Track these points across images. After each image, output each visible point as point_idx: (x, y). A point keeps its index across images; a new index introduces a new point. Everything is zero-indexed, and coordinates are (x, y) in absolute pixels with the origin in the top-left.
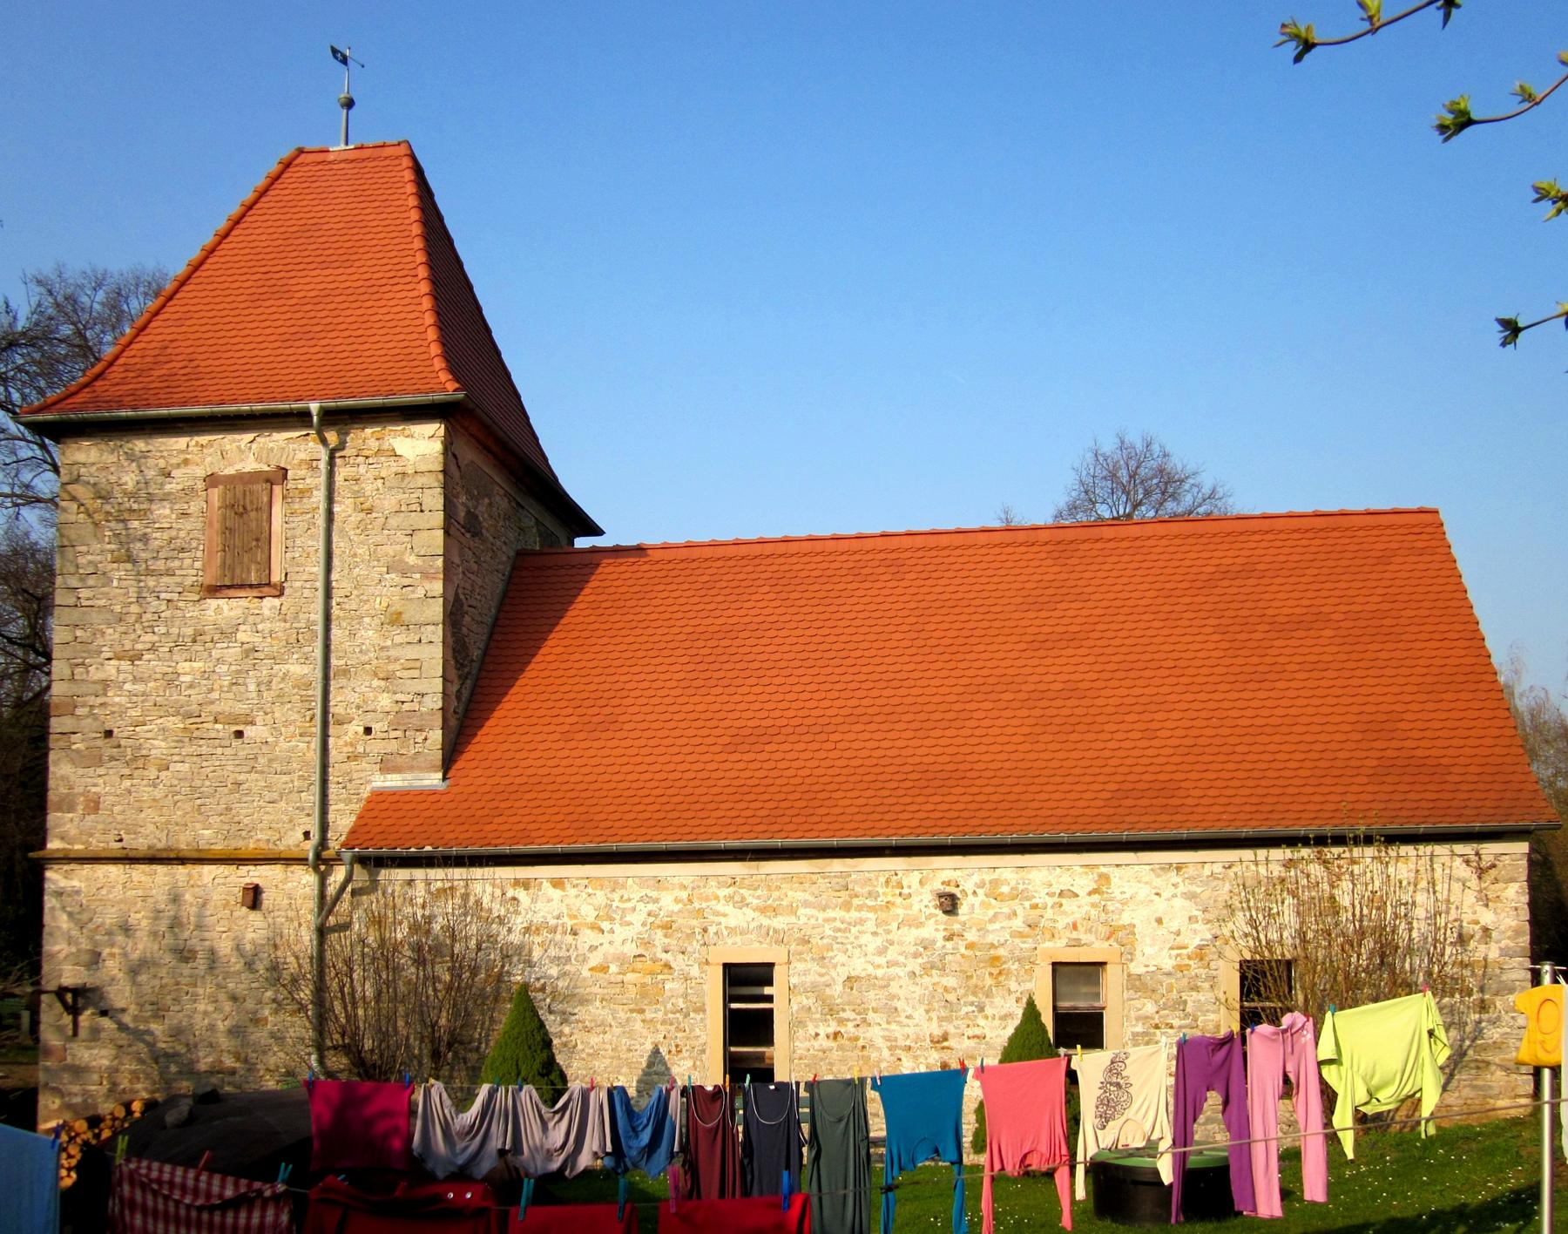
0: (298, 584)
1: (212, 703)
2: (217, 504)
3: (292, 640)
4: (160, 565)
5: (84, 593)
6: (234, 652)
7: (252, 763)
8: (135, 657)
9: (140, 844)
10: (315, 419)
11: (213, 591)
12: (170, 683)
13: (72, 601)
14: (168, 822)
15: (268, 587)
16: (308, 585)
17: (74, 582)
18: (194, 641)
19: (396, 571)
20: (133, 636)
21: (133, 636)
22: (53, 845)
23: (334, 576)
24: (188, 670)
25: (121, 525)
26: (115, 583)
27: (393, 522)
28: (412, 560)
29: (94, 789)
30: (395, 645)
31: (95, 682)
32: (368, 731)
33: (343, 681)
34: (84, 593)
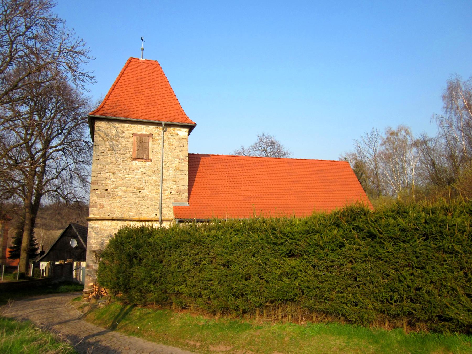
0: (155, 160)
1: (134, 184)
2: (136, 140)
3: (154, 172)
4: (121, 152)
5: (101, 157)
6: (139, 173)
7: (144, 198)
8: (114, 173)
9: (115, 216)
10: (163, 125)
11: (135, 159)
12: (123, 179)
13: (98, 158)
14: (122, 211)
15: (147, 159)
16: (157, 160)
17: (98, 154)
18: (129, 170)
19: (178, 159)
20: (113, 168)
21: (113, 168)
22: (91, 216)
23: (164, 159)
24: (128, 176)
25: (111, 142)
26: (109, 155)
27: (177, 148)
28: (181, 157)
29: (102, 203)
30: (178, 175)
31: (103, 178)
32: (171, 192)
33: (165, 182)
34: (101, 157)
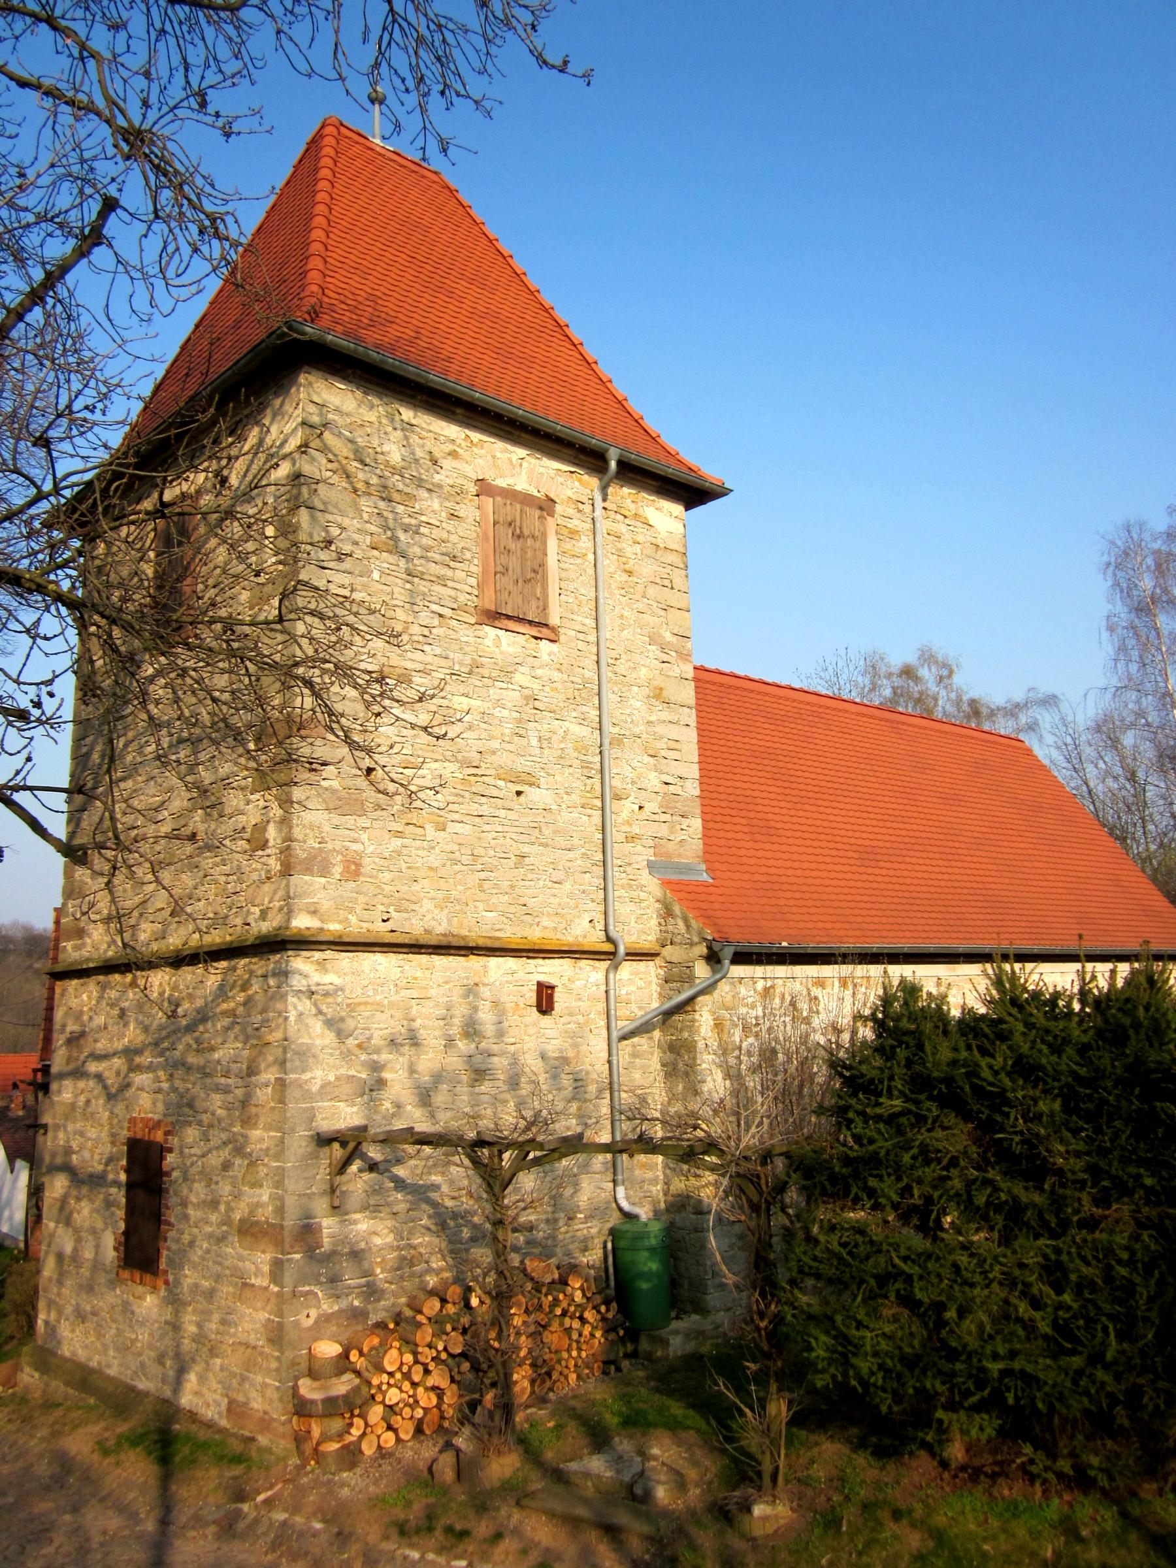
1: (494, 753)
6: (513, 697)
9: (414, 927)
11: (494, 617)
15: (542, 629)
26: (376, 575)
27: (652, 591)
28: (668, 637)
33: (616, 753)
